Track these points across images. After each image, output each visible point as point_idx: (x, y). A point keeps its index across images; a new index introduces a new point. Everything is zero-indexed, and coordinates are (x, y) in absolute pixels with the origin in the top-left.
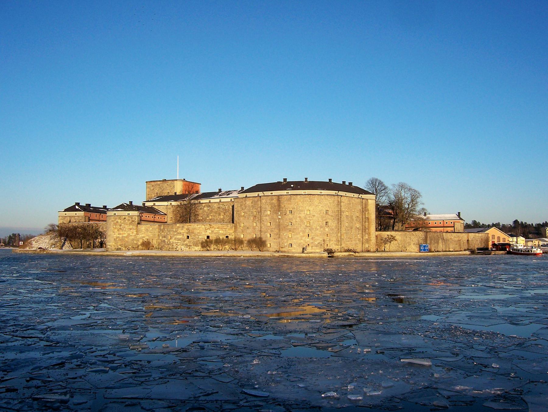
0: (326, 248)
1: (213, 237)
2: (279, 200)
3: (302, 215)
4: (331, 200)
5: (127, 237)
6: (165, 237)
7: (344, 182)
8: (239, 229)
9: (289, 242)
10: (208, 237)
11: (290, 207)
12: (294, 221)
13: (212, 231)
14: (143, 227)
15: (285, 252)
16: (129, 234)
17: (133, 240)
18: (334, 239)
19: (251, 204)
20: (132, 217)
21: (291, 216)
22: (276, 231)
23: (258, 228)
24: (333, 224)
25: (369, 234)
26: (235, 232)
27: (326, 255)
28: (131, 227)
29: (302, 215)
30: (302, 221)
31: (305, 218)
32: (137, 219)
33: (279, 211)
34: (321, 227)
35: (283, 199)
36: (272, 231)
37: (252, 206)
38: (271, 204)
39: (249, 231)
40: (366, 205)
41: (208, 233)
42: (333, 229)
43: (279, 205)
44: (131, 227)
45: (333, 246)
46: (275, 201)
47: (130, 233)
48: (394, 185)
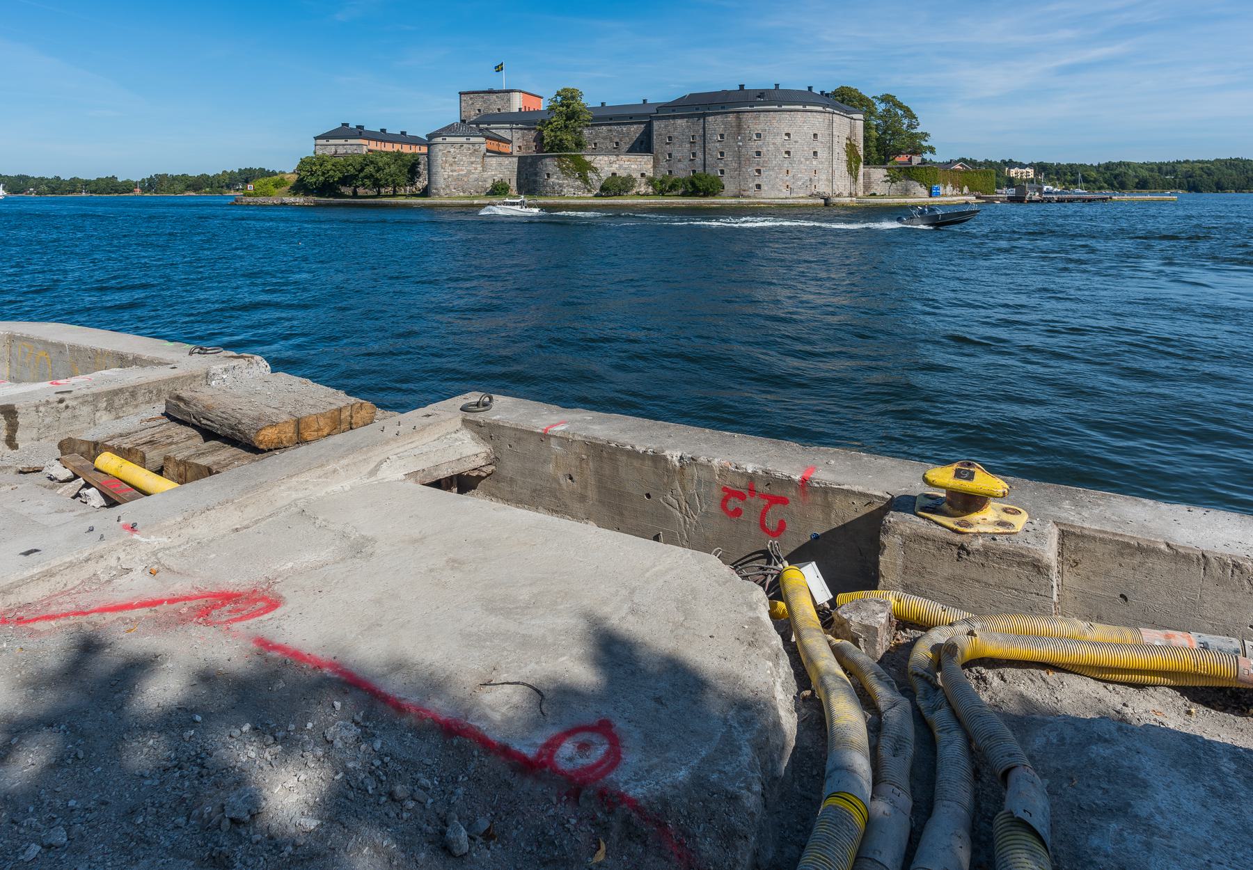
1: (622, 174)
2: (738, 118)
3: (778, 141)
9: (757, 182)
11: (759, 128)
13: (621, 166)
14: (493, 161)
16: (469, 172)
17: (477, 180)
20: (473, 144)
21: (760, 143)
23: (699, 160)
26: (654, 167)
28: (473, 159)
29: (778, 141)
30: (778, 150)
31: (783, 145)
32: (483, 148)
33: (739, 134)
34: (807, 159)
35: (745, 115)
38: (725, 123)
39: (680, 165)
41: (614, 168)
43: (739, 126)
44: (473, 159)
47: (471, 168)
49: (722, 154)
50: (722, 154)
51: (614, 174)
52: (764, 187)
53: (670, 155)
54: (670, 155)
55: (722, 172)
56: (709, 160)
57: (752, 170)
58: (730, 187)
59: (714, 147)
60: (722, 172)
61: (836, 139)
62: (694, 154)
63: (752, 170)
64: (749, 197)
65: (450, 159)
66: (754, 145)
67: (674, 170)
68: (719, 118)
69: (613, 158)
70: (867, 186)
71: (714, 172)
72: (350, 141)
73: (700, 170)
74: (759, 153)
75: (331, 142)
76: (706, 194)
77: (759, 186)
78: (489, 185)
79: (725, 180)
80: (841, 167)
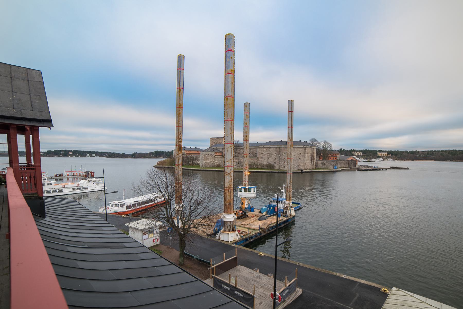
0: (299, 168)
4: (302, 149)
8: (260, 160)
15: (282, 170)
22: (278, 161)
24: (302, 159)
32: (214, 155)
35: (281, 149)
40: (313, 150)
43: (280, 151)
45: (302, 167)
46: (278, 149)
58: (277, 167)
59: (273, 156)
70: (316, 166)
71: (273, 163)
73: (269, 162)
76: (271, 169)
79: (276, 165)
80: (308, 162)
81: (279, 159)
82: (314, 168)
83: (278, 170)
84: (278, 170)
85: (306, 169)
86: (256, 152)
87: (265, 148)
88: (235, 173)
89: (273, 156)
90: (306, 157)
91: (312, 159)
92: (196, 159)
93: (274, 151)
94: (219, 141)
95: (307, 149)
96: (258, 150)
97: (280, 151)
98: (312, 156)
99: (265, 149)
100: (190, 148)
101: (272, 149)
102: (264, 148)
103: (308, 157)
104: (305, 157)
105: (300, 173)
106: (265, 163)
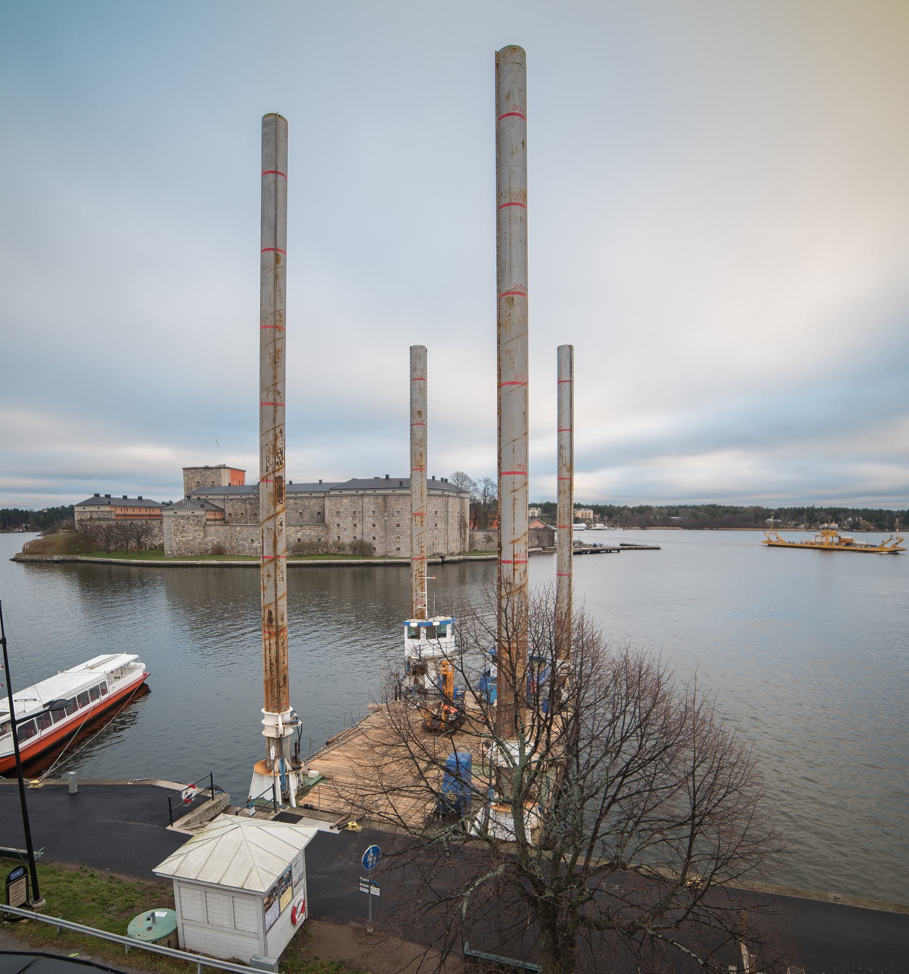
0: (436, 551)
1: (306, 540)
4: (439, 500)
5: (192, 540)
6: (244, 540)
7: (442, 479)
8: (334, 530)
10: (299, 540)
11: (399, 507)
12: (402, 523)
13: (304, 534)
15: (392, 557)
16: (195, 538)
18: (442, 542)
19: (348, 504)
20: (197, 517)
22: (382, 534)
25: (465, 533)
27: (440, 560)
28: (197, 528)
32: (204, 519)
35: (389, 499)
36: (377, 534)
37: (351, 505)
39: (346, 533)
40: (464, 503)
41: (299, 535)
42: (440, 532)
43: (385, 506)
44: (197, 528)
45: (441, 549)
46: (380, 500)
48: (480, 481)
49: (374, 525)
50: (374, 525)
51: (299, 540)
52: (402, 550)
53: (338, 525)
54: (338, 525)
55: (374, 538)
56: (366, 530)
57: (393, 537)
58: (380, 550)
59: (369, 521)
60: (374, 538)
61: (450, 515)
62: (355, 525)
63: (393, 537)
64: (392, 557)
65: (181, 528)
66: (395, 520)
67: (341, 536)
68: (372, 500)
69: (298, 528)
70: (472, 544)
71: (368, 539)
72: (102, 509)
73: (359, 537)
74: (398, 525)
75: (88, 509)
77: (398, 549)
78: (209, 546)
80: (454, 533)
81: (385, 528)
82: (467, 550)
83: (384, 557)
84: (384, 557)
85: (452, 554)
86: (320, 510)
87: (346, 496)
88: (290, 570)
89: (369, 521)
90: (451, 521)
91: (462, 526)
92: (147, 531)
93: (369, 504)
94: (211, 477)
95: (450, 500)
96: (328, 503)
97: (385, 506)
98: (462, 518)
99: (345, 501)
100: (140, 498)
101: (366, 500)
102: (341, 496)
103: (454, 522)
104: (447, 522)
105: (439, 564)
106: (347, 538)
